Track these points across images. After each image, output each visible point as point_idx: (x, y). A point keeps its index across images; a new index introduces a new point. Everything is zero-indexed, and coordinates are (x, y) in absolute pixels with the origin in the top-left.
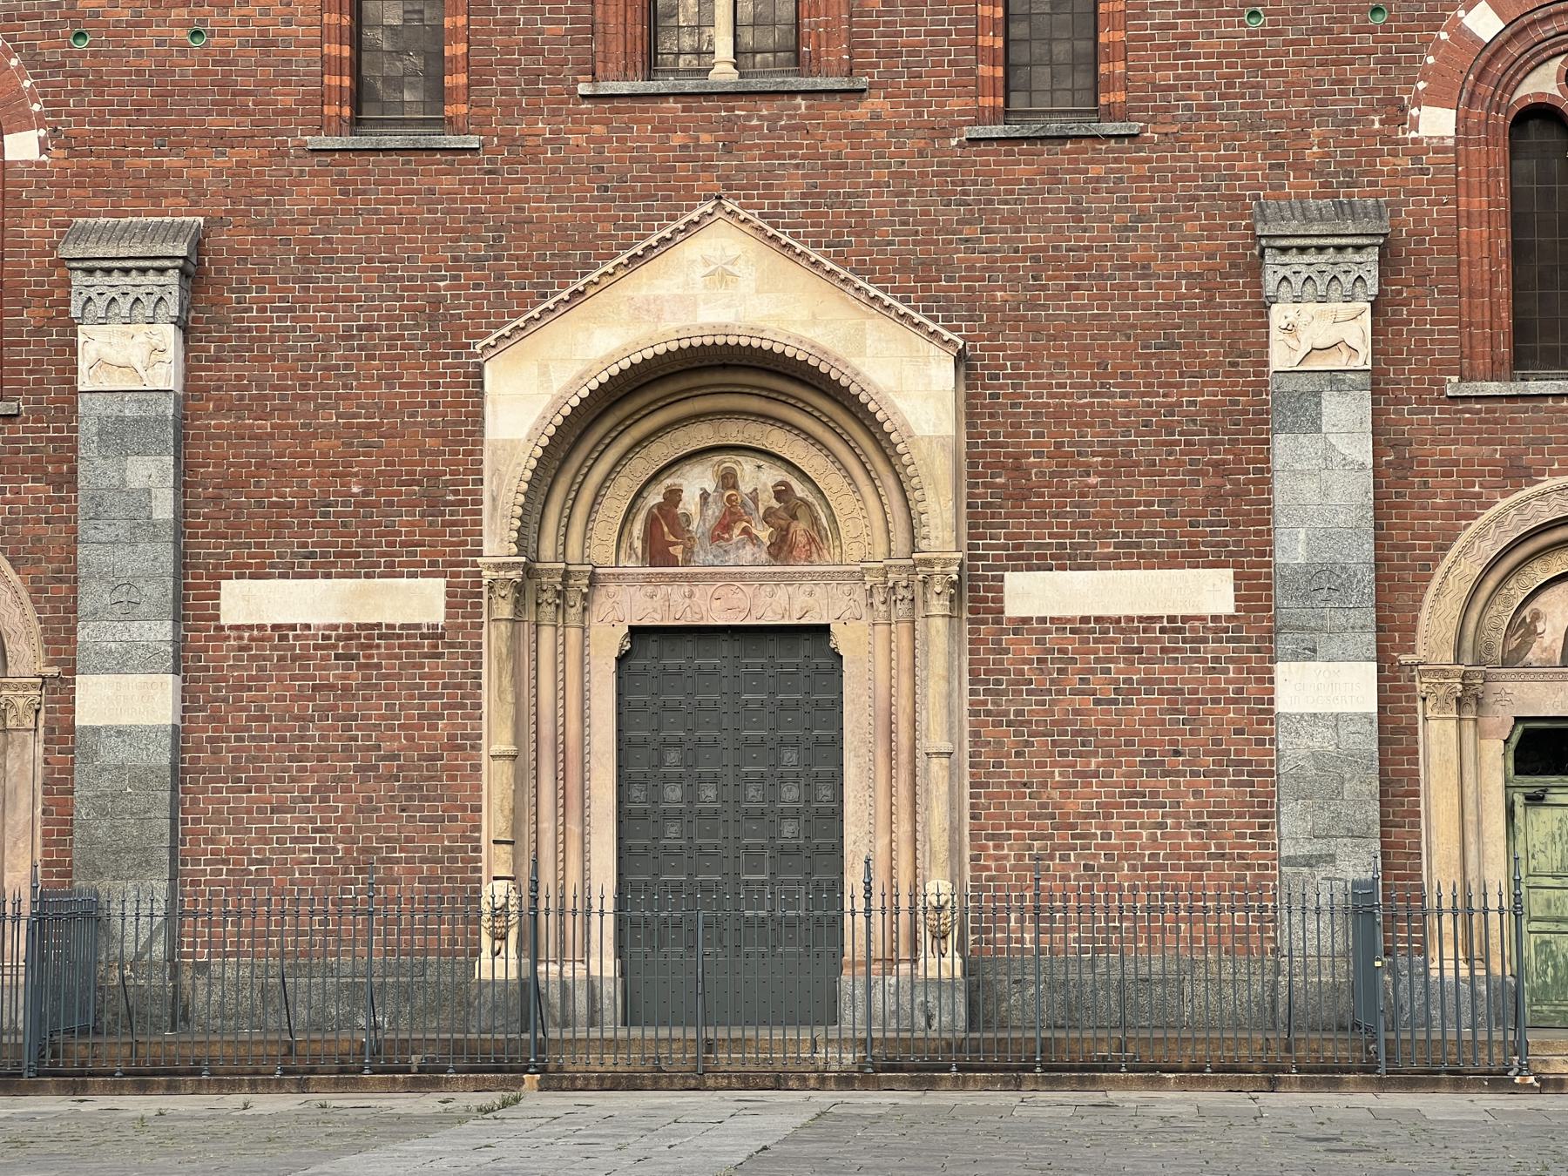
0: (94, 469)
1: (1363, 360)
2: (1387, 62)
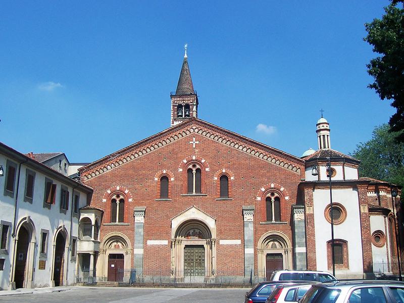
0: (136, 229)
2: (254, 193)
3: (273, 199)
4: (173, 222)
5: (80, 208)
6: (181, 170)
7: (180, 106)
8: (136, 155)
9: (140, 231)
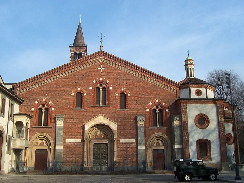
1: (144, 126)
3: (157, 111)
4: (85, 126)
5: (14, 114)
6: (91, 88)
7: (76, 54)
8: (58, 76)
9: (60, 132)
